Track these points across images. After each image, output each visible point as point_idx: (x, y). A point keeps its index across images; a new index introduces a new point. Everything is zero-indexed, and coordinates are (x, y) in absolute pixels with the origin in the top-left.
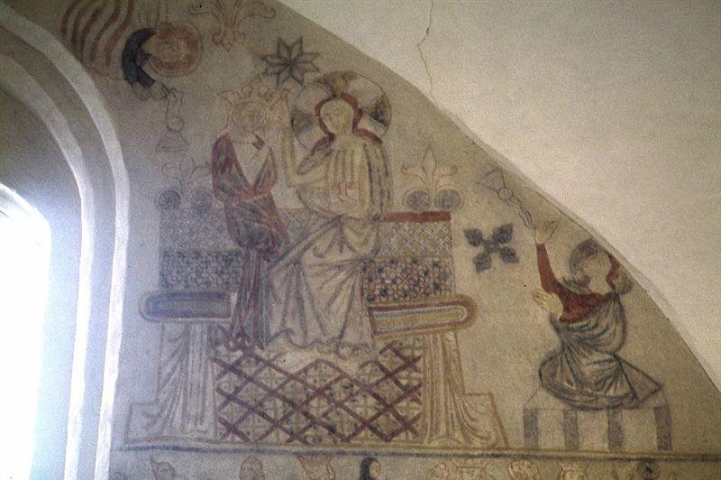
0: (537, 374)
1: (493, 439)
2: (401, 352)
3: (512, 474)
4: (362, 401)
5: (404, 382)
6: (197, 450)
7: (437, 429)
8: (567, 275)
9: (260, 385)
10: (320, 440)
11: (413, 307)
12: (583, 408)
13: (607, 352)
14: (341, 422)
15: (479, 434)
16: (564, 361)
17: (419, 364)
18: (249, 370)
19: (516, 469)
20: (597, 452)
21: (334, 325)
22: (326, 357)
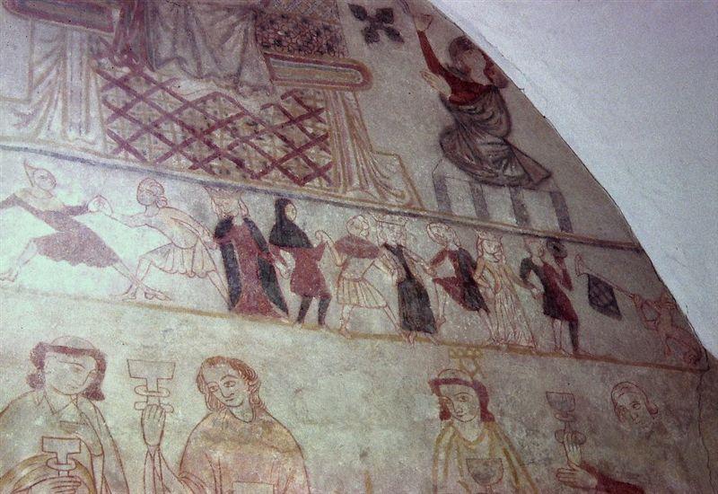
1: (408, 199)
2: (303, 100)
3: (432, 235)
4: (269, 141)
5: (310, 130)
6: (83, 161)
7: (351, 181)
8: (450, 62)
9: (152, 105)
10: (228, 172)
11: (308, 62)
12: (486, 183)
13: (496, 136)
15: (392, 191)
16: (460, 136)
17: (323, 115)
18: (141, 89)
20: (508, 225)
21: (231, 61)
22: (224, 91)
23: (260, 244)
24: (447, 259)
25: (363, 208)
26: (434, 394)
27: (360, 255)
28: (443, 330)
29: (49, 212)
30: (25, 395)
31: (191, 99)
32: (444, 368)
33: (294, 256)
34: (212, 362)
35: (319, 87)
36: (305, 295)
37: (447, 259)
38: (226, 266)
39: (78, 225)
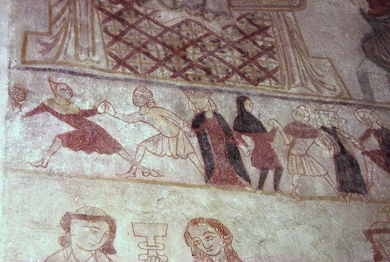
0: (361, 47)
1: (339, 91)
2: (254, 21)
4: (229, 53)
5: (260, 43)
6: (92, 76)
7: (294, 80)
9: (141, 32)
10: (200, 79)
14: (215, 67)
16: (378, 40)
17: (270, 31)
18: (132, 20)
19: (361, 115)
22: (193, 18)
23: (227, 131)
24: (372, 136)
25: (304, 100)
26: (368, 242)
27: (304, 135)
28: (373, 192)
29: (68, 115)
30: (58, 252)
31: (169, 25)
32: (375, 220)
33: (253, 139)
34: (195, 222)
35: (265, 10)
36: (263, 169)
37: (372, 136)
38: (202, 148)
39: (90, 124)
